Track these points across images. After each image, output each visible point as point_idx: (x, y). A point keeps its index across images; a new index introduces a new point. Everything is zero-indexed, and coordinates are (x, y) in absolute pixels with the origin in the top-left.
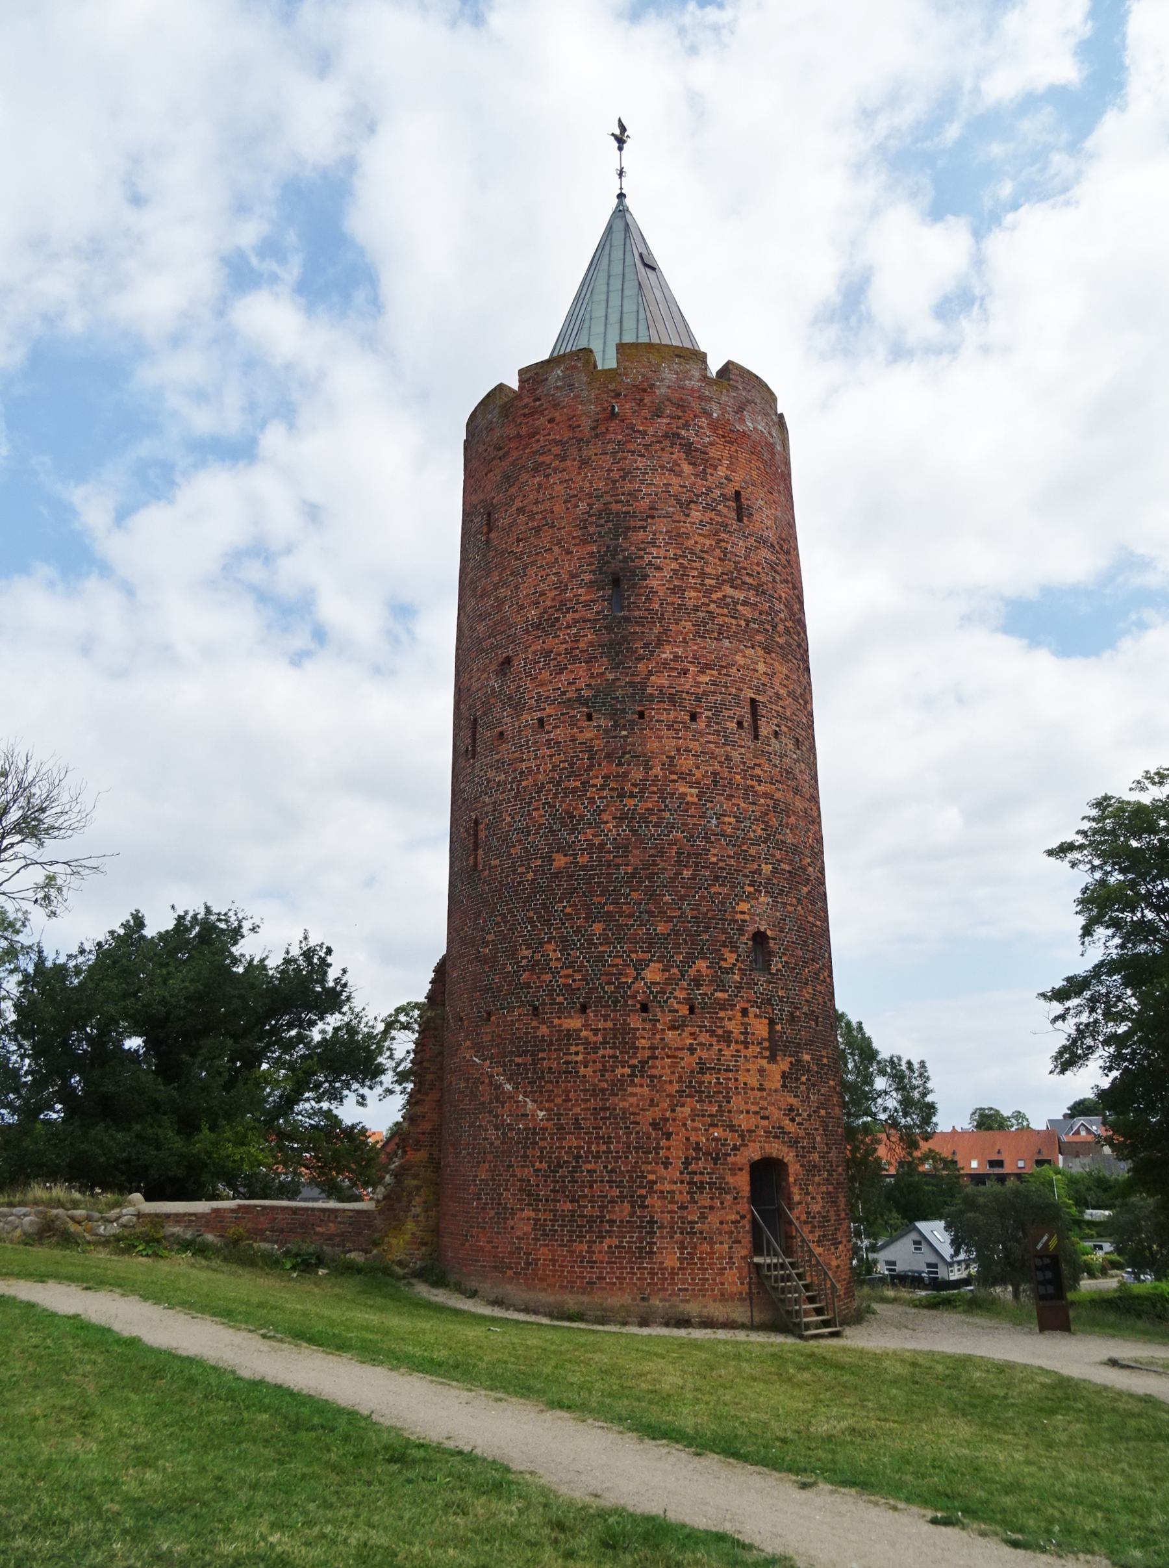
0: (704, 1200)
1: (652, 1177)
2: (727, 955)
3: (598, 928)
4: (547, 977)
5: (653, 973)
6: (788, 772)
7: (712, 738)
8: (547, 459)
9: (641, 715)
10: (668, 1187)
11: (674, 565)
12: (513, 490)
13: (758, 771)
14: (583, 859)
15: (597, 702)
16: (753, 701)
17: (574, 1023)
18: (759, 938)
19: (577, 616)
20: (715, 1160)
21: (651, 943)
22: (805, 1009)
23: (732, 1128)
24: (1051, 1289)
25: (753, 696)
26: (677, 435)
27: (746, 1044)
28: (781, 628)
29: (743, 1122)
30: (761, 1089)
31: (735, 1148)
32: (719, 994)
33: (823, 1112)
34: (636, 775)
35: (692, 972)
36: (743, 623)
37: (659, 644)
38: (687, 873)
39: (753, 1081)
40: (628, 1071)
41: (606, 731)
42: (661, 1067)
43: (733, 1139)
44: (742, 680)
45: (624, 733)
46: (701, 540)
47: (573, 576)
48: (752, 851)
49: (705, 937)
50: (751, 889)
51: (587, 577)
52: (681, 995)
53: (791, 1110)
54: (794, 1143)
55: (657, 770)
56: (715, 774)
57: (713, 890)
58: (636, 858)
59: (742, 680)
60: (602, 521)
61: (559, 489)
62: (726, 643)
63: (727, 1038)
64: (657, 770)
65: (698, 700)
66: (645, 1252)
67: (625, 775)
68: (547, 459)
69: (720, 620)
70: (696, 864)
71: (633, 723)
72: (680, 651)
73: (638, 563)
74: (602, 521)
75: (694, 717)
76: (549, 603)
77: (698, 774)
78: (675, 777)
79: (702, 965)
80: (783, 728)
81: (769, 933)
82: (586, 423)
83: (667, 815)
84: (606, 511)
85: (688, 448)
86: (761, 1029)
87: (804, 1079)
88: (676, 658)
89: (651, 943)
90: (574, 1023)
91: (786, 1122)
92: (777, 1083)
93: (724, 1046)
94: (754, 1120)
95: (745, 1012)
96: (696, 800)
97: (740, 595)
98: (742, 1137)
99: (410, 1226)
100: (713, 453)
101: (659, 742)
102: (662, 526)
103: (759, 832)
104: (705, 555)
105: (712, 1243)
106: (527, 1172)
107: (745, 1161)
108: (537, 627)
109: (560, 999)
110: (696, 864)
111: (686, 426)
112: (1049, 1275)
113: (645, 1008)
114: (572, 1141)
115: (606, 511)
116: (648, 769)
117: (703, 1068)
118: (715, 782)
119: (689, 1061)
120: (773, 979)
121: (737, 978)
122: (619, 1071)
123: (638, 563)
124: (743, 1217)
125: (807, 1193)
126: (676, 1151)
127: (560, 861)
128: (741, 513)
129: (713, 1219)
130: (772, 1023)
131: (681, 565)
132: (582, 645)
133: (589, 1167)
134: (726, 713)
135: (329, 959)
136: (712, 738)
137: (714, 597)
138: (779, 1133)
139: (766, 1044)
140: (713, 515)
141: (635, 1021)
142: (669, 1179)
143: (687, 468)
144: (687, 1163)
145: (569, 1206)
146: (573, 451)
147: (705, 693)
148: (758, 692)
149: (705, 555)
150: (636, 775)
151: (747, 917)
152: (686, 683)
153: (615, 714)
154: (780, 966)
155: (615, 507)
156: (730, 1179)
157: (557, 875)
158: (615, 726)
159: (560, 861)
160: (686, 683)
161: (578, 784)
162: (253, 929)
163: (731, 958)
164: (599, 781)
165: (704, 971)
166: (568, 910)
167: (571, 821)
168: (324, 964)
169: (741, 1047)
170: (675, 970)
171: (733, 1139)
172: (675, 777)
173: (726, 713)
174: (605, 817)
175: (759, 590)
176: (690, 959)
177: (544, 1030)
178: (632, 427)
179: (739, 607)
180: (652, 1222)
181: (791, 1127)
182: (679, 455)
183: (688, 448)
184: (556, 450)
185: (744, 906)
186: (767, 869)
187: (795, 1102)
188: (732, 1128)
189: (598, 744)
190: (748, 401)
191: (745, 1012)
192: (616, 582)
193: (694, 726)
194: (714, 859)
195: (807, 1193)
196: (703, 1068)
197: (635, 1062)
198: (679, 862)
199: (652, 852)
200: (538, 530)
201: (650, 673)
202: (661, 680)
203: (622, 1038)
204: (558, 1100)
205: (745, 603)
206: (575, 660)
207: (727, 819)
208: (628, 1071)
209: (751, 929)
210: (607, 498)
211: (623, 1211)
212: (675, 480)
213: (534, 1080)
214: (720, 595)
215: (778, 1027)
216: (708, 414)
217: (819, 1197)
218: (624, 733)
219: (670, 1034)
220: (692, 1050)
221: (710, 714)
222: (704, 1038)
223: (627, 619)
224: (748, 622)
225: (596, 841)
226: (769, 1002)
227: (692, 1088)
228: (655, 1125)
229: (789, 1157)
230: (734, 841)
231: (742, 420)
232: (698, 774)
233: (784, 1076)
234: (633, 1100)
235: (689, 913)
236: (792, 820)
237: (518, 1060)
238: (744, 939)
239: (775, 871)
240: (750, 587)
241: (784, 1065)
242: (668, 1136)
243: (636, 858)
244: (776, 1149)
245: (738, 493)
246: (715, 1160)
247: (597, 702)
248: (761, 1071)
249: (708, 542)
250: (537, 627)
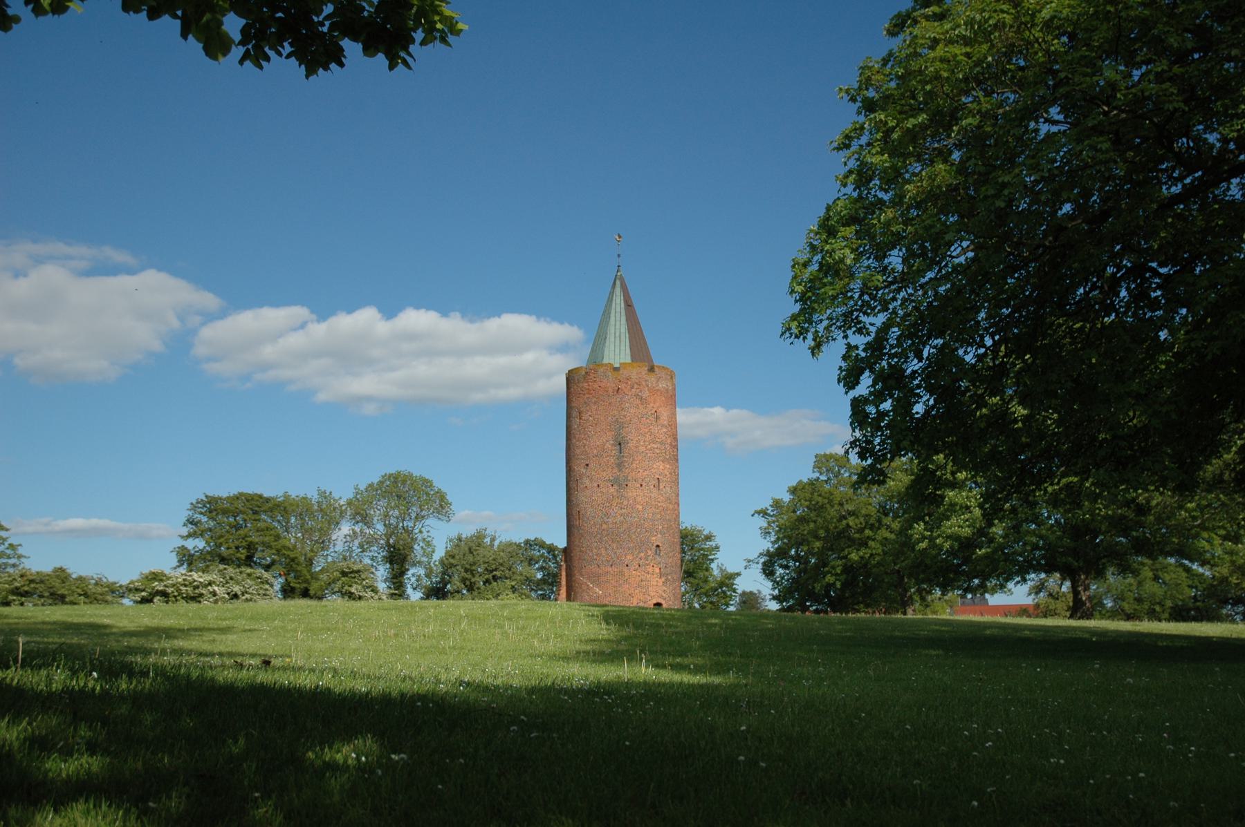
5: (630, 557)
34: (625, 503)
58: (625, 526)
86: (657, 570)
101: (633, 492)
119: (638, 579)
127: (604, 526)
128: (657, 418)
138: (661, 597)
141: (625, 569)
150: (625, 503)
153: (620, 485)
182: (638, 402)
213: (598, 585)
243: (625, 526)
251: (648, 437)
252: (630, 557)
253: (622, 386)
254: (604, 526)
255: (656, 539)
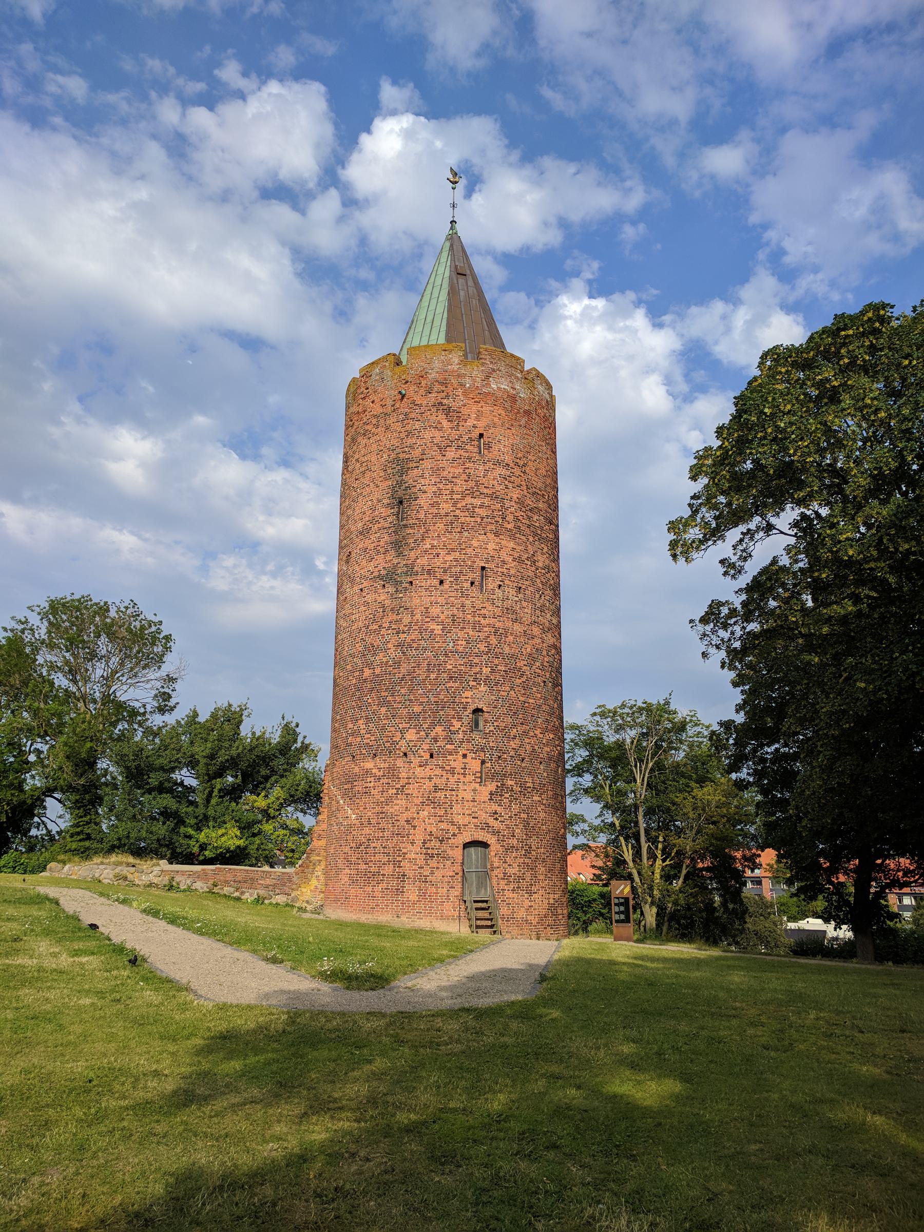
0: (433, 863)
1: (404, 851)
2: (455, 722)
3: (383, 710)
4: (359, 739)
5: (411, 735)
6: (508, 609)
7: (453, 594)
8: (369, 427)
9: (411, 583)
10: (413, 856)
11: (434, 489)
12: (355, 447)
13: (483, 612)
14: (378, 671)
15: (389, 578)
16: (483, 568)
17: (369, 765)
18: (477, 711)
19: (380, 526)
20: (441, 841)
21: (411, 717)
22: (512, 753)
23: (453, 823)
24: (622, 917)
25: (483, 565)
26: (441, 404)
27: (464, 774)
28: (510, 518)
29: (461, 820)
30: (474, 801)
31: (454, 835)
32: (448, 746)
33: (522, 815)
35: (433, 734)
36: (479, 520)
37: (423, 540)
38: (433, 676)
39: (468, 796)
40: (395, 791)
41: (392, 595)
42: (412, 789)
43: (453, 829)
44: (476, 556)
45: (401, 595)
46: (452, 470)
47: (379, 501)
48: (476, 660)
49: (441, 713)
50: (475, 683)
51: (386, 501)
52: (426, 747)
53: (496, 813)
54: (496, 833)
55: (418, 617)
56: (453, 616)
57: (448, 685)
59: (476, 556)
60: (394, 466)
61: (374, 447)
62: (466, 534)
63: (452, 772)
64: (418, 617)
65: (445, 571)
66: (400, 891)
67: (401, 620)
68: (369, 427)
69: (463, 519)
70: (439, 670)
71: (406, 589)
72: (435, 543)
73: (413, 490)
74: (394, 466)
75: (441, 582)
76: (367, 519)
77: (442, 617)
78: (428, 620)
79: (439, 729)
80: (507, 582)
81: (485, 709)
82: (389, 403)
83: (422, 642)
84: (397, 459)
85: (448, 411)
86: (475, 765)
87: (507, 795)
88: (433, 546)
89: (411, 717)
90: (369, 765)
91: (491, 821)
92: (485, 796)
93: (450, 776)
94: (467, 819)
95: (465, 756)
96: (440, 632)
97: (477, 502)
98: (459, 828)
99: (314, 882)
100: (465, 411)
102: (427, 464)
103: (482, 648)
104: (453, 480)
105: (437, 888)
106: (347, 849)
107: (461, 842)
108: (361, 533)
109: (364, 751)
110: (439, 670)
111: (447, 396)
112: (622, 908)
113: (405, 754)
114: (367, 831)
115: (397, 459)
116: (413, 615)
117: (436, 789)
118: (454, 620)
119: (429, 785)
120: (486, 735)
121: (461, 736)
122: (390, 791)
123: (413, 490)
124: (457, 874)
125: (505, 862)
126: (419, 836)
129: (438, 874)
130: (483, 762)
131: (439, 489)
132: (382, 543)
133: (374, 845)
134: (463, 578)
135: (297, 730)
136: (453, 594)
137: (459, 506)
139: (478, 775)
140: (461, 452)
141: (400, 763)
142: (413, 852)
143: (445, 423)
144: (424, 843)
145: (365, 867)
146: (382, 421)
147: (450, 567)
148: (488, 561)
149: (453, 480)
150: (406, 619)
151: (469, 700)
152: (438, 562)
153: (397, 583)
154: (492, 728)
155: (402, 456)
156: (450, 852)
157: (365, 680)
158: (396, 591)
159: (367, 672)
160: (438, 562)
161: (376, 627)
162: (249, 716)
163: (457, 725)
164: (386, 625)
165: (440, 733)
166: (369, 701)
167: (372, 649)
168: (296, 734)
169: (461, 777)
170: (422, 733)
171: (453, 829)
172: (428, 620)
173: (463, 578)
174: (390, 646)
175: (494, 496)
176: (433, 726)
177: (357, 769)
178: (413, 402)
179: (477, 510)
180: (404, 875)
181: (496, 824)
182: (441, 417)
183: (448, 411)
184: (374, 421)
185: (468, 694)
186: (486, 671)
187: (499, 809)
188: (453, 823)
189: (388, 603)
190: (494, 370)
191: (465, 756)
192: (401, 502)
193: (441, 588)
194: (450, 667)
195: (505, 862)
196: (436, 789)
197: (398, 786)
198: (428, 670)
199: (413, 665)
200: (364, 473)
201: (417, 558)
202: (423, 561)
203: (392, 773)
204: (361, 809)
205: (481, 507)
206: (378, 552)
207: (460, 642)
208: (395, 791)
209: (473, 707)
210: (398, 450)
211: (388, 870)
212: (437, 434)
213: (351, 796)
214: (464, 504)
215: (489, 765)
216: (462, 385)
217: (515, 865)
218: (401, 595)
219: (418, 769)
220: (430, 778)
221: (452, 579)
222: (438, 772)
223: (405, 526)
224: (482, 518)
225: (385, 660)
226: (482, 750)
227: (430, 801)
228: (407, 821)
229: (491, 840)
230: (464, 654)
231: (488, 385)
232: (442, 617)
233: (491, 794)
234: (396, 807)
235: (433, 699)
236: (511, 638)
237: (346, 787)
238: (466, 713)
239: (493, 671)
240: (487, 495)
241: (492, 786)
242: (415, 827)
244: (481, 836)
245: (481, 435)
246: (441, 841)
247: (389, 578)
248: (474, 790)
249: (457, 471)
250: (361, 533)
251: (461, 485)
252: (411, 735)
253: (411, 390)
254: (367, 672)
255: (477, 696)
